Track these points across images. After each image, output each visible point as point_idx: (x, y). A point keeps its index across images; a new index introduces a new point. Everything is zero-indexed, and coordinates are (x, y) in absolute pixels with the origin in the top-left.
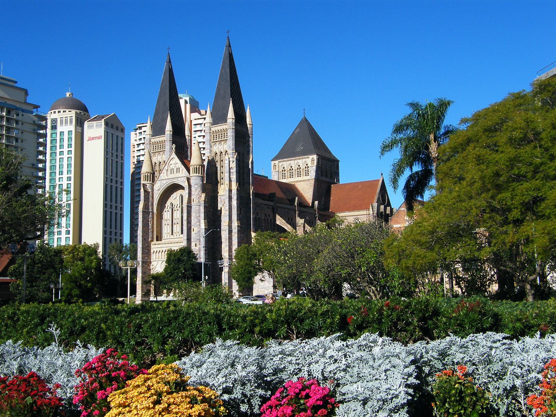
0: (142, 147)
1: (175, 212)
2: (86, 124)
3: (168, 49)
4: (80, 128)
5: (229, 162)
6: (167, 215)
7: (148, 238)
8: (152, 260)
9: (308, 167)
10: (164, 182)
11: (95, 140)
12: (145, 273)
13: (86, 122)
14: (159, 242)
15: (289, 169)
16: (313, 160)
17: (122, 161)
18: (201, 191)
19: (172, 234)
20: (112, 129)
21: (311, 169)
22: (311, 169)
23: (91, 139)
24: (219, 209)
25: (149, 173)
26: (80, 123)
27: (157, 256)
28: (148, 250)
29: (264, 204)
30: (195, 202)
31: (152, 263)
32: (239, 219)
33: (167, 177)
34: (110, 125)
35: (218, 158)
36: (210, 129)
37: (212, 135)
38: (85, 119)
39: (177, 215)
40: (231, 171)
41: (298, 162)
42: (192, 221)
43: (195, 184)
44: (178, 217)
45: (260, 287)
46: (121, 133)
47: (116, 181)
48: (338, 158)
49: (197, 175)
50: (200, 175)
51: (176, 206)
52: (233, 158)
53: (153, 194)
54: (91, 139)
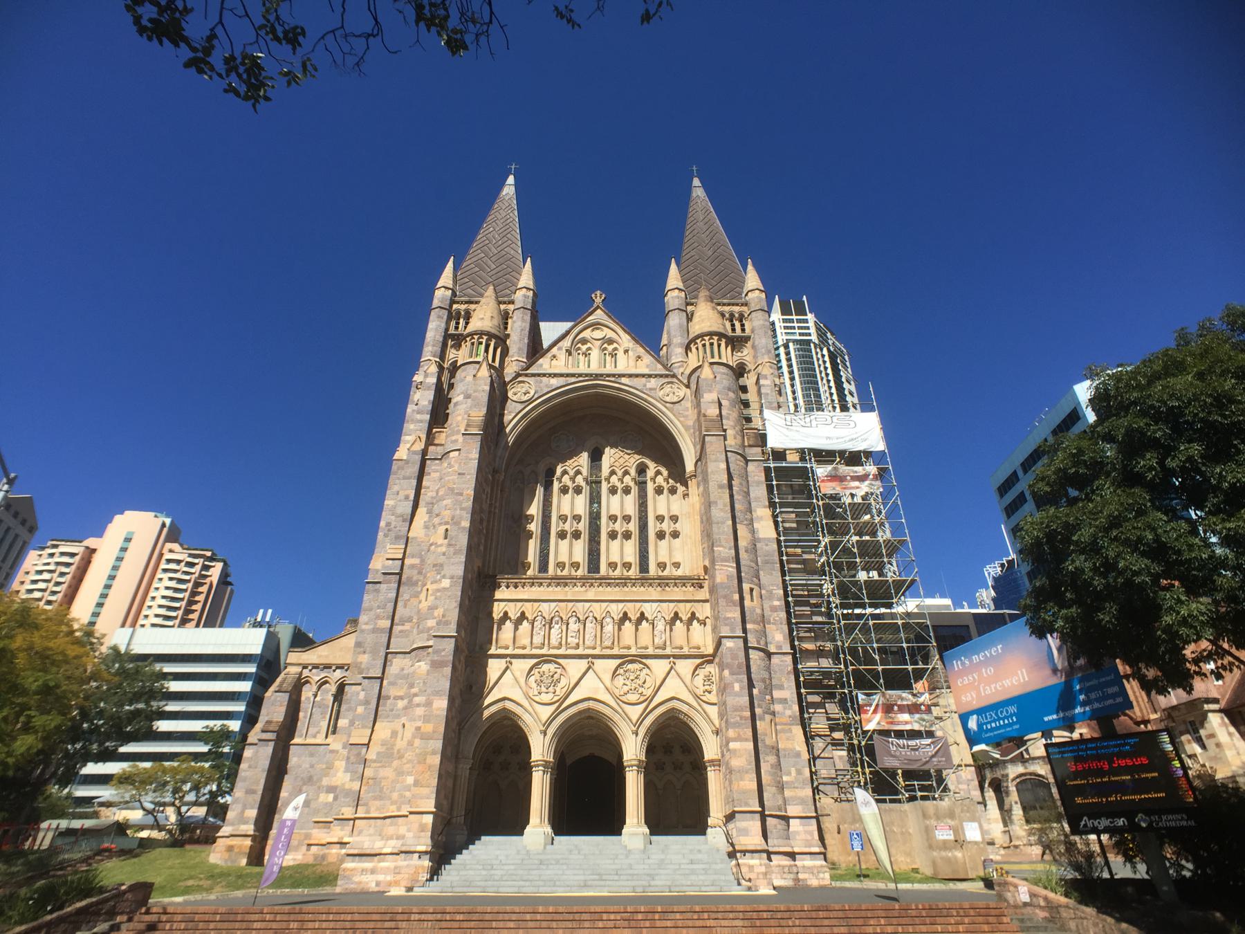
10: (555, 382)
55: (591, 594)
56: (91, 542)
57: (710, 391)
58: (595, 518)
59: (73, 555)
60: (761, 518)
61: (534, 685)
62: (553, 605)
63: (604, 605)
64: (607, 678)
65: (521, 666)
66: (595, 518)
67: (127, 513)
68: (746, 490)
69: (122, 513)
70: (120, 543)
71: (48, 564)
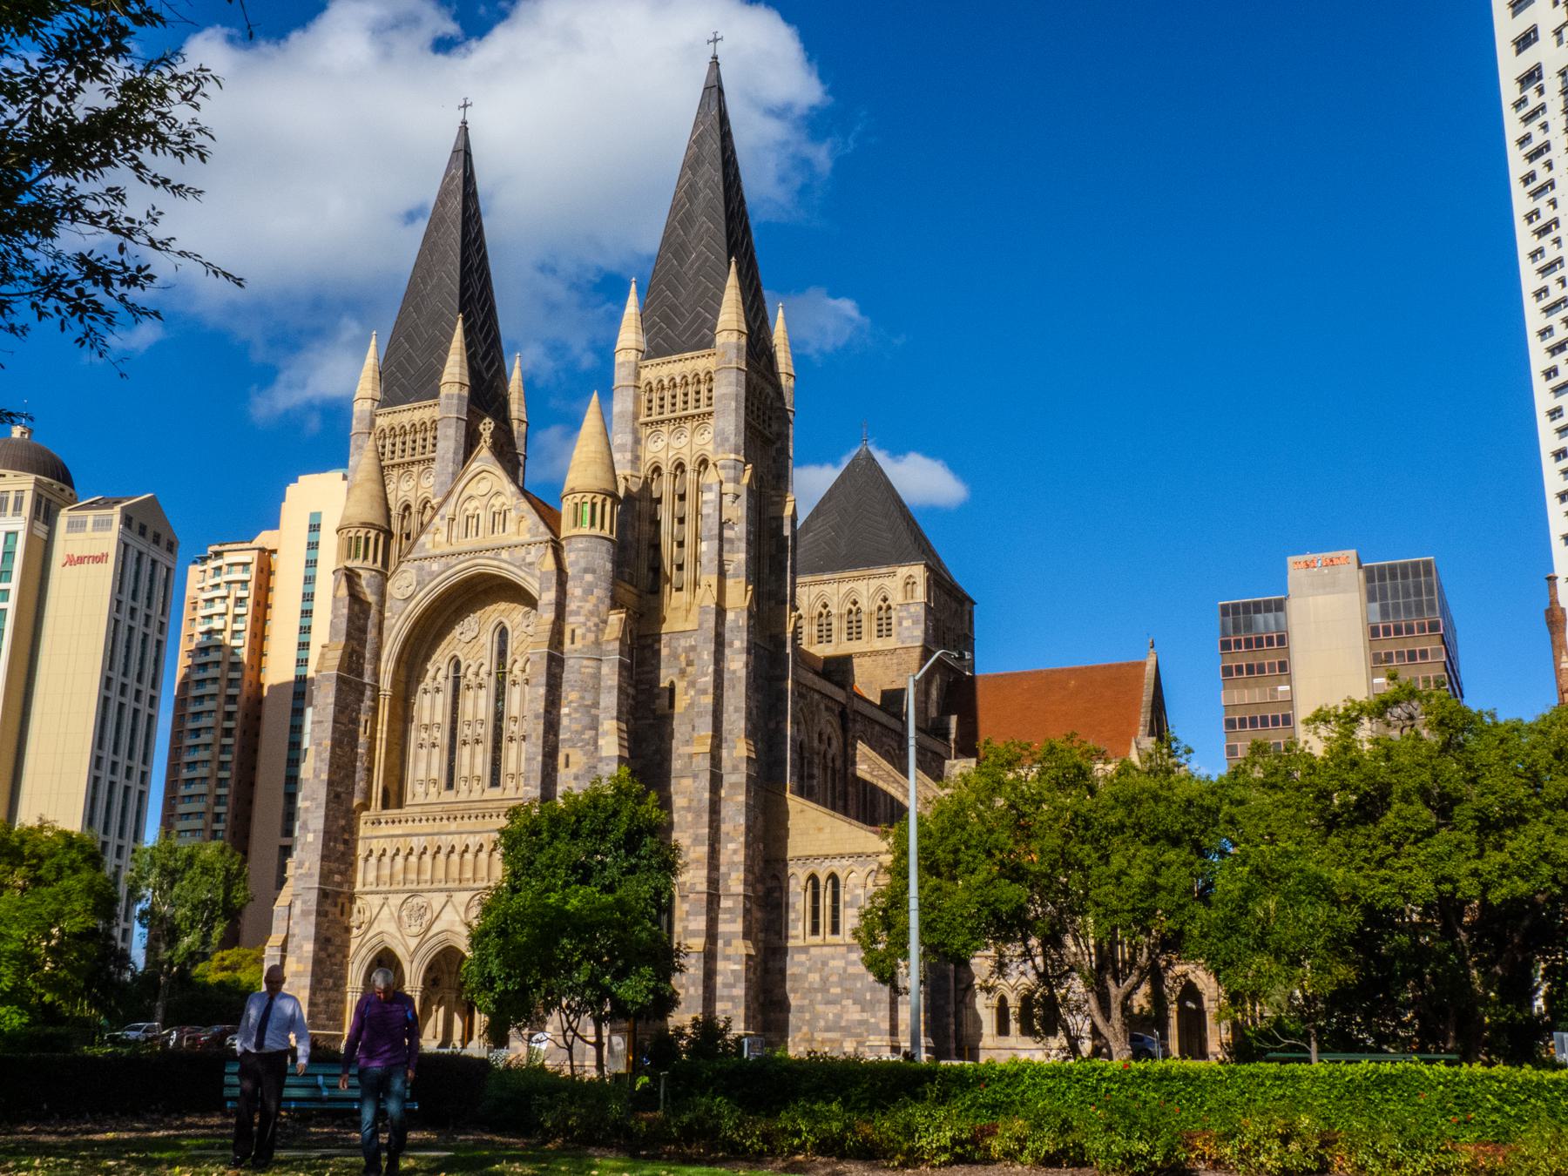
0: (219, 607)
1: (471, 693)
2: (64, 518)
3: (465, 106)
4: (45, 528)
5: (721, 495)
6: (433, 707)
7: (351, 794)
8: (358, 887)
9: (889, 608)
10: (435, 567)
11: (84, 567)
12: (328, 940)
13: (64, 511)
14: (393, 813)
15: (816, 613)
16: (909, 583)
17: (159, 637)
18: (608, 601)
19: (450, 785)
20: (141, 539)
21: (905, 614)
22: (905, 614)
23: (73, 561)
24: (664, 683)
25: (371, 526)
26: (45, 512)
27: (386, 872)
28: (346, 842)
29: (819, 692)
30: (578, 644)
31: (359, 902)
32: (751, 734)
33: (447, 549)
34: (135, 525)
35: (664, 487)
36: (637, 375)
37: (644, 398)
38: (59, 501)
39: (475, 705)
40: (727, 533)
41: (852, 590)
42: (565, 722)
43: (586, 570)
44: (481, 715)
45: (822, 1023)
46: (167, 555)
47: (138, 692)
48: (970, 591)
49: (596, 531)
50: (606, 532)
51: (471, 670)
52: (737, 481)
53: (381, 613)
54: (73, 561)
55: (453, 826)
56: (265, 539)
57: (548, 589)
58: (499, 716)
59: (246, 565)
60: (606, 733)
61: (406, 919)
62: (422, 839)
63: (464, 836)
64: (462, 910)
65: (395, 900)
66: (499, 716)
67: (301, 478)
68: (588, 702)
69: (296, 481)
70: (303, 536)
71: (217, 586)
